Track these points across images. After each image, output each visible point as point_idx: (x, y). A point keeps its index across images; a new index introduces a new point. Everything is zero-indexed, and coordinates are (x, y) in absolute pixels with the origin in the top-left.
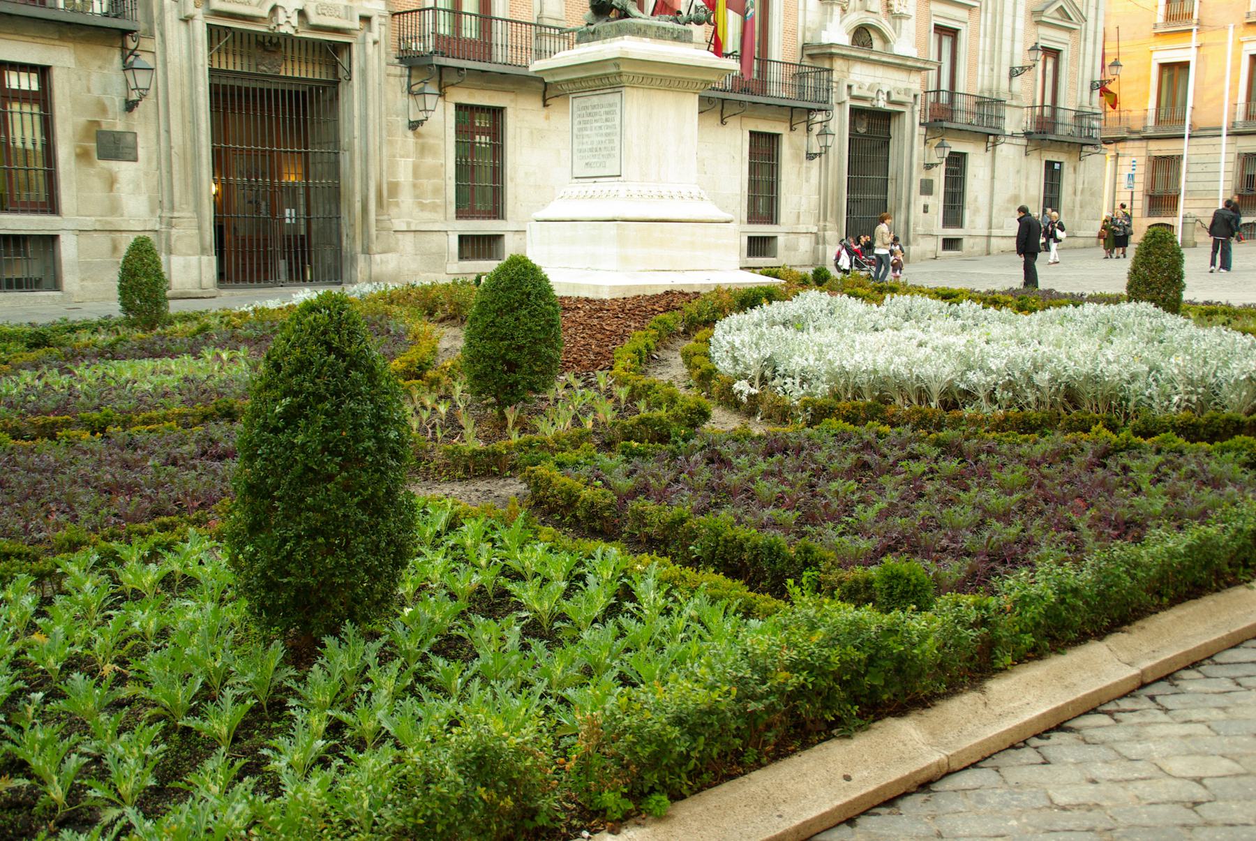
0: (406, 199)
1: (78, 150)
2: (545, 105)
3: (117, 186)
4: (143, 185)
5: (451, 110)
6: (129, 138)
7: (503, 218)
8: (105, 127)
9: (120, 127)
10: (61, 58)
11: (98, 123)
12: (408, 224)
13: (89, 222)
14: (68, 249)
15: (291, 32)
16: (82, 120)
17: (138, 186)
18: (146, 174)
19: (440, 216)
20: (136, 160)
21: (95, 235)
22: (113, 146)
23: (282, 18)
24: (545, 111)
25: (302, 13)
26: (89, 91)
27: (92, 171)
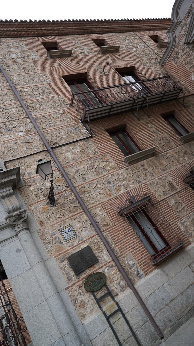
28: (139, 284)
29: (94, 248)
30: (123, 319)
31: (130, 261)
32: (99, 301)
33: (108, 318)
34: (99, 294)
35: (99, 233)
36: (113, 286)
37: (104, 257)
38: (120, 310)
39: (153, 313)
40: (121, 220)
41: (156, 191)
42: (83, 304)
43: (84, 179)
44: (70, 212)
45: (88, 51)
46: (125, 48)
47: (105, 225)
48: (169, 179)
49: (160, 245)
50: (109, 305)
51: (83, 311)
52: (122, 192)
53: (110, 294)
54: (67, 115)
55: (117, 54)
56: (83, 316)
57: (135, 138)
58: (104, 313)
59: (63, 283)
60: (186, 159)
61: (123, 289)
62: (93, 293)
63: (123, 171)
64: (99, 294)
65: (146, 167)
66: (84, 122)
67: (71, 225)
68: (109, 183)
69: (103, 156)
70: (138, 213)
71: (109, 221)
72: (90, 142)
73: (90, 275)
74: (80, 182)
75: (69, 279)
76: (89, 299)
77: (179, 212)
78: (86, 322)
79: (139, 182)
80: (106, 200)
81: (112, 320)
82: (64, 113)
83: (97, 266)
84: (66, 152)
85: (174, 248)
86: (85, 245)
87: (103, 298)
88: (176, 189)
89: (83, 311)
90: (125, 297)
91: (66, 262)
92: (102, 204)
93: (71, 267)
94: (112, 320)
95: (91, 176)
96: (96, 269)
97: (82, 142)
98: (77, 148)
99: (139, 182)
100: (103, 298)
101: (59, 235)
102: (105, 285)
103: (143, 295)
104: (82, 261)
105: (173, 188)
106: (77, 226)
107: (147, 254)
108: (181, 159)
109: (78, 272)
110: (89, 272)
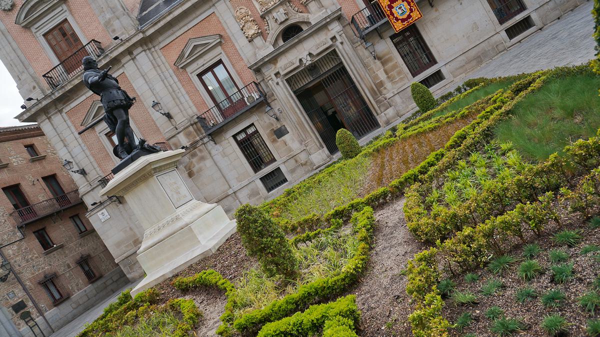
0: (388, 85)
1: (272, 140)
2: (432, 7)
3: (287, 144)
4: (295, 139)
5: (389, 40)
6: (283, 128)
7: (526, 9)
8: (275, 129)
9: (279, 127)
10: (254, 119)
11: (273, 129)
12: (393, 92)
13: (284, 159)
14: (283, 169)
15: (310, 62)
16: (268, 131)
17: (293, 139)
18: (293, 134)
19: (406, 81)
20: (288, 133)
21: (289, 161)
22: (280, 133)
23: (304, 61)
24: (434, 9)
25: (310, 54)
26: (266, 122)
27: (278, 144)
28: (46, 314)
29: (24, 300)
30: (37, 328)
31: (42, 305)
32: (27, 323)
33: (31, 328)
34: (27, 320)
35: (28, 294)
36: (33, 316)
37: (30, 304)
38: (37, 324)
39: (51, 324)
40: (39, 286)
41: (59, 270)
42: (19, 324)
43: (19, 266)
44: (12, 284)
45: (21, 159)
46: (50, 154)
47: (30, 290)
48: (68, 262)
49: (57, 296)
50: (31, 323)
51: (19, 327)
52: (40, 271)
53: (32, 319)
54: (8, 222)
55: (43, 161)
56: (19, 329)
57: (50, 235)
58: (29, 326)
59: (10, 317)
60: (80, 248)
61: (38, 317)
62: (24, 319)
63: (41, 259)
64: (27, 320)
65: (55, 255)
66: (20, 228)
67: (13, 291)
68: (34, 267)
69: (31, 250)
70: (49, 282)
71: (32, 286)
72: (24, 244)
73: (23, 313)
74: (18, 268)
75: (13, 315)
76: (22, 322)
77: (70, 280)
78: (21, 330)
79: (50, 265)
80: (31, 276)
81: (33, 328)
82: (5, 221)
83: (26, 309)
84: (8, 250)
85: (65, 298)
86: (21, 300)
87: (28, 321)
88: (71, 267)
89: (19, 327)
90: (39, 320)
91: (11, 308)
92: (30, 279)
93: (14, 310)
94: (33, 328)
95: (24, 264)
96: (26, 310)
97: (18, 242)
98: (15, 247)
99: (50, 265)
100: (28, 321)
101: (6, 296)
102: (30, 316)
103: (47, 318)
104: (18, 307)
105: (69, 266)
106: (16, 291)
107: (50, 301)
108: (77, 249)
109: (17, 312)
110: (22, 311)
